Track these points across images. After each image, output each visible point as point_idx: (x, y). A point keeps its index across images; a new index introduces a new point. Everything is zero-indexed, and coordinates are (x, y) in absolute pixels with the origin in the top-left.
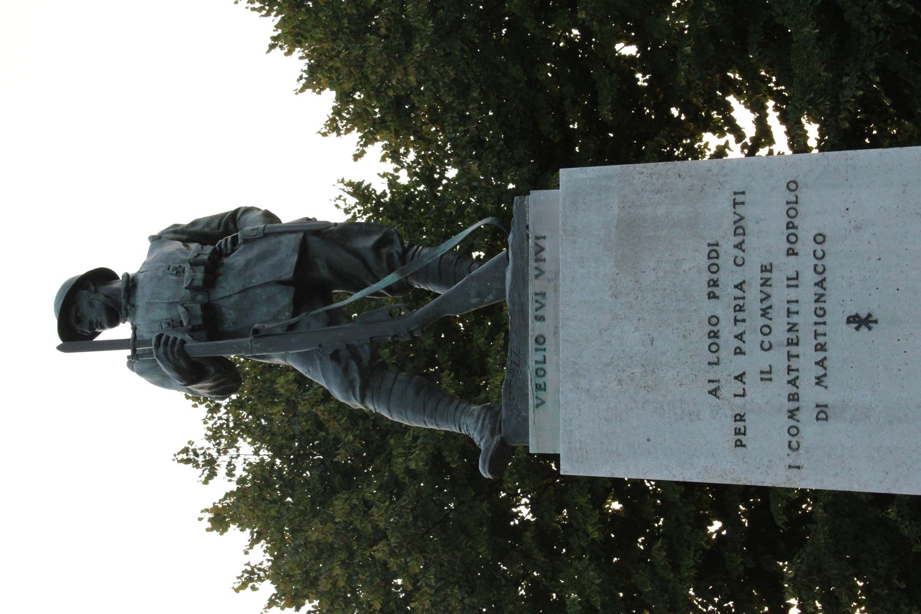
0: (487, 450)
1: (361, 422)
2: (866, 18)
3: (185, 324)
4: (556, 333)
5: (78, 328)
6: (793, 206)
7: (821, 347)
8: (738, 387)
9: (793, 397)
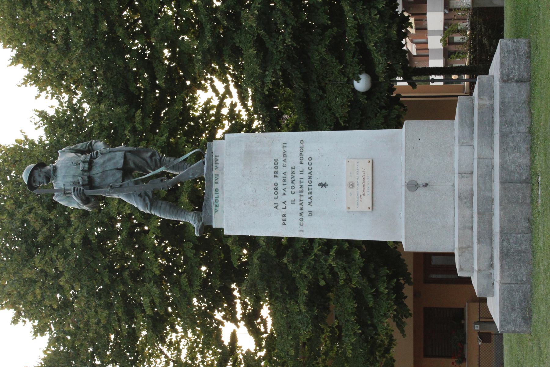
0: (198, 227)
1: (49, 222)
2: (275, 46)
3: (81, 183)
4: (222, 188)
5: (34, 184)
6: (302, 148)
7: (310, 193)
8: (284, 206)
9: (301, 209)
